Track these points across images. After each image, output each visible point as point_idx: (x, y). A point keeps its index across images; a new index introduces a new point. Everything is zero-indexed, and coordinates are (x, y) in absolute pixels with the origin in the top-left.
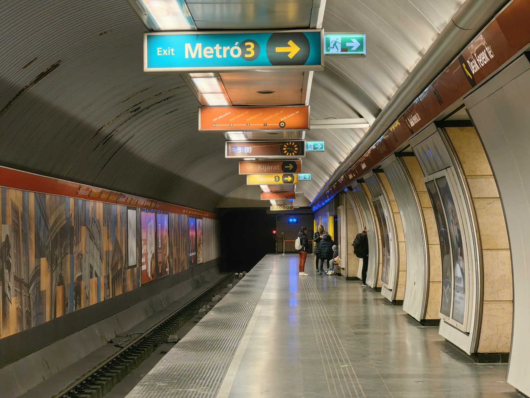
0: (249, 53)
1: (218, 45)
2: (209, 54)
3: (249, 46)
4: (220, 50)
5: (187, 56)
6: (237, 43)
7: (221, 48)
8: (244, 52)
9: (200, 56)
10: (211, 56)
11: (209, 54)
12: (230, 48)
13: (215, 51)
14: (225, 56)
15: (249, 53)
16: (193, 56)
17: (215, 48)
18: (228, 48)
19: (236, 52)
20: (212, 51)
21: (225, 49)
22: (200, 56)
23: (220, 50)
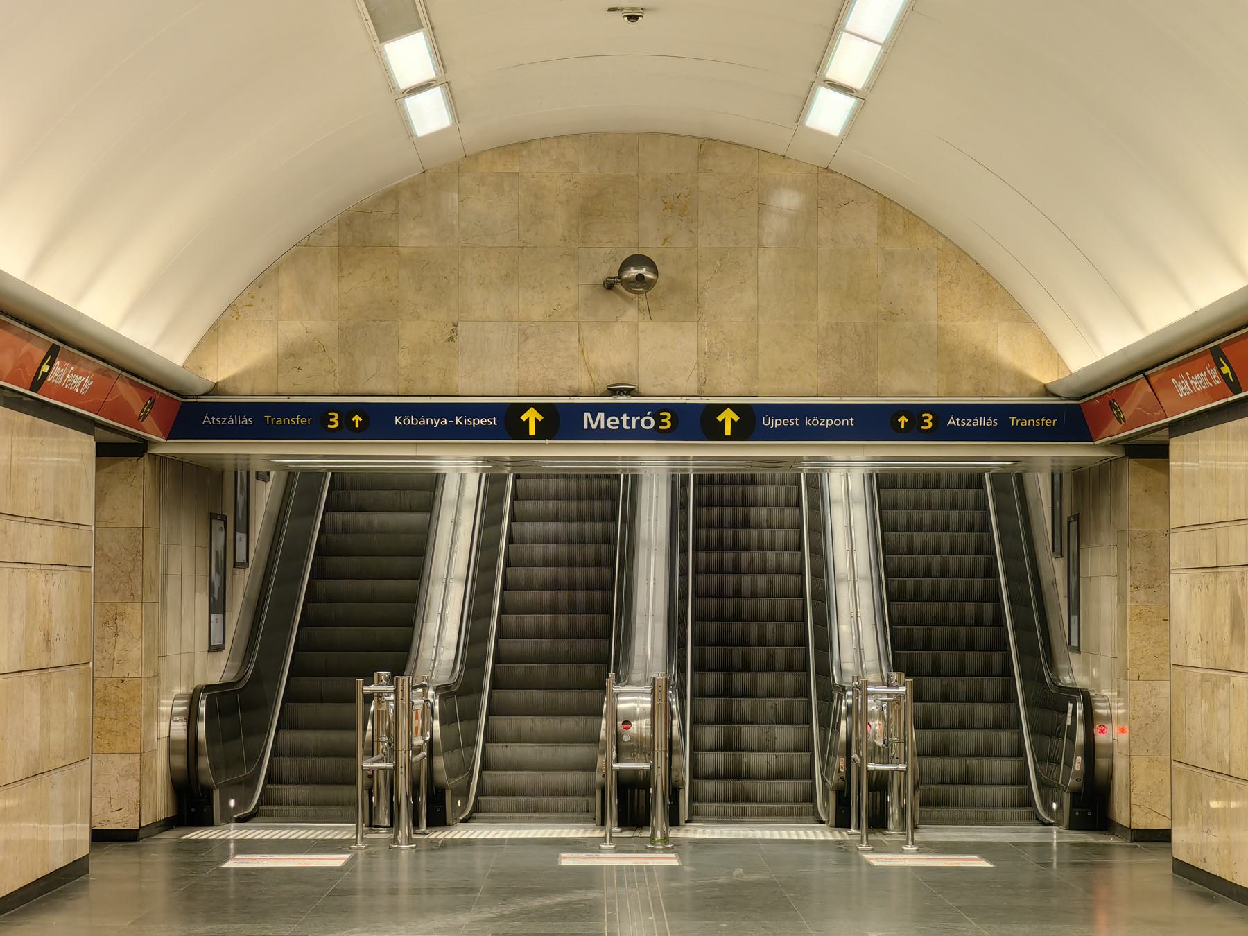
0: (665, 424)
1: (625, 415)
2: (612, 425)
3: (665, 417)
4: (627, 420)
5: (586, 427)
6: (649, 413)
7: (628, 418)
8: (659, 422)
9: (602, 427)
10: (617, 427)
11: (612, 425)
12: (641, 418)
13: (621, 421)
14: (634, 427)
15: (665, 424)
16: (594, 426)
17: (621, 418)
18: (638, 418)
19: (648, 423)
20: (617, 422)
21: (634, 420)
22: (602, 427)
23: (627, 420)
